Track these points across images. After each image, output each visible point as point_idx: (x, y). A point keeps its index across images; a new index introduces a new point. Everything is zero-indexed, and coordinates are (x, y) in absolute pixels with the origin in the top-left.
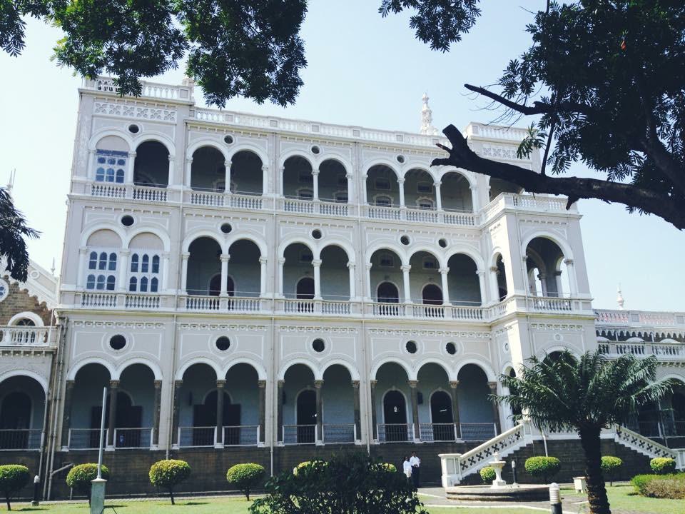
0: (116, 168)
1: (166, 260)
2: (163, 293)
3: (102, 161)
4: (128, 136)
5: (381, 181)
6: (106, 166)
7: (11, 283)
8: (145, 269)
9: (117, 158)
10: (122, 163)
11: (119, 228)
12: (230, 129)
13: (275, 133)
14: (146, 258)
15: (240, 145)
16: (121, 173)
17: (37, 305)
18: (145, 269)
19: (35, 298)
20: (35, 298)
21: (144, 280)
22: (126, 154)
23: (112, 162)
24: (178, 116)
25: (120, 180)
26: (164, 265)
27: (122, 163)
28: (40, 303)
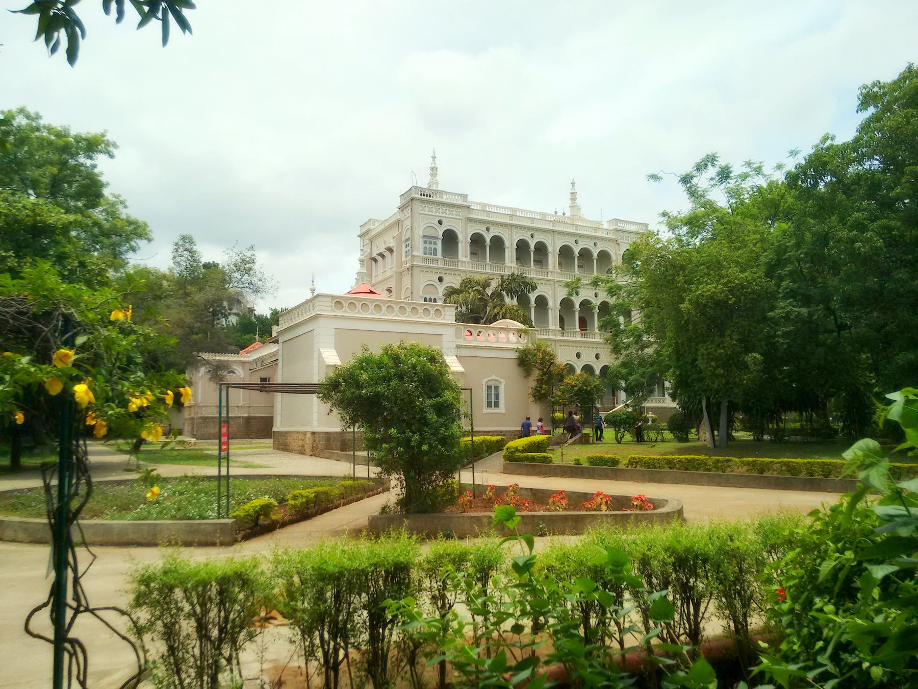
0: (433, 246)
3: (425, 242)
4: (437, 226)
5: (565, 253)
6: (428, 246)
9: (433, 241)
10: (435, 243)
11: (437, 284)
12: (489, 222)
13: (512, 225)
15: (494, 232)
16: (435, 249)
22: (437, 238)
23: (430, 243)
24: (463, 214)
25: (435, 254)
27: (435, 243)
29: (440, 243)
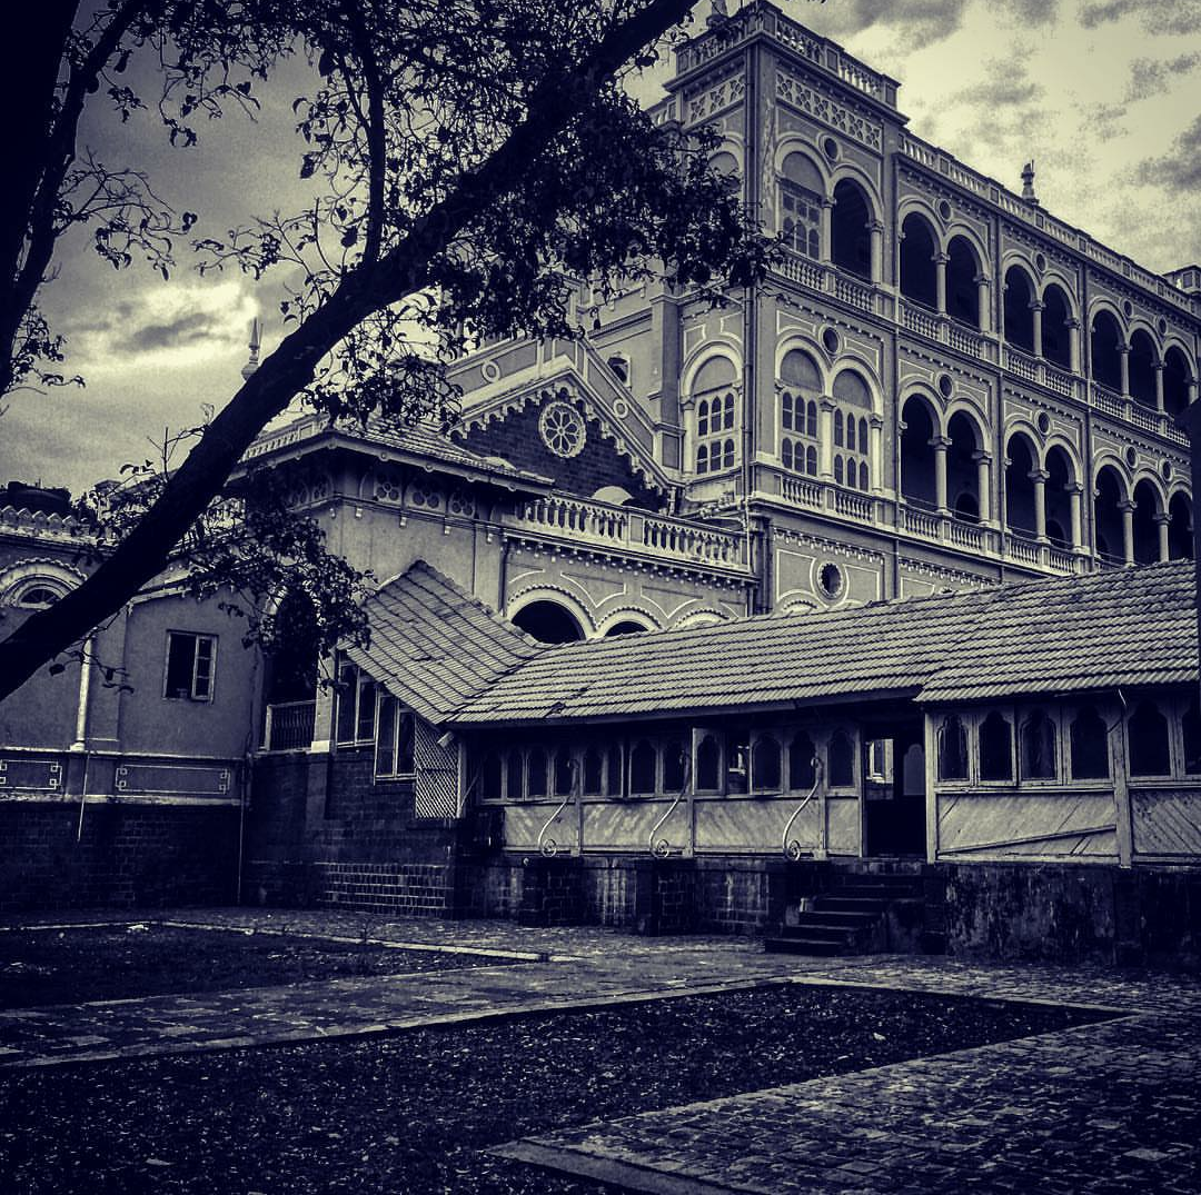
1: (876, 431)
2: (878, 494)
3: (787, 203)
7: (590, 419)
8: (851, 446)
10: (814, 217)
14: (851, 417)
16: (814, 237)
17: (629, 473)
18: (851, 446)
19: (626, 458)
20: (626, 458)
21: (851, 463)
22: (819, 200)
26: (876, 440)
28: (635, 471)
29: (826, 216)
